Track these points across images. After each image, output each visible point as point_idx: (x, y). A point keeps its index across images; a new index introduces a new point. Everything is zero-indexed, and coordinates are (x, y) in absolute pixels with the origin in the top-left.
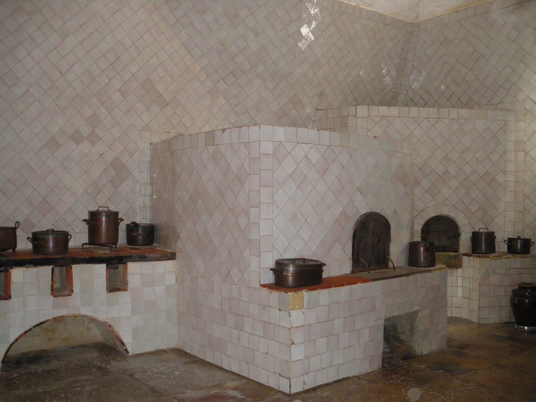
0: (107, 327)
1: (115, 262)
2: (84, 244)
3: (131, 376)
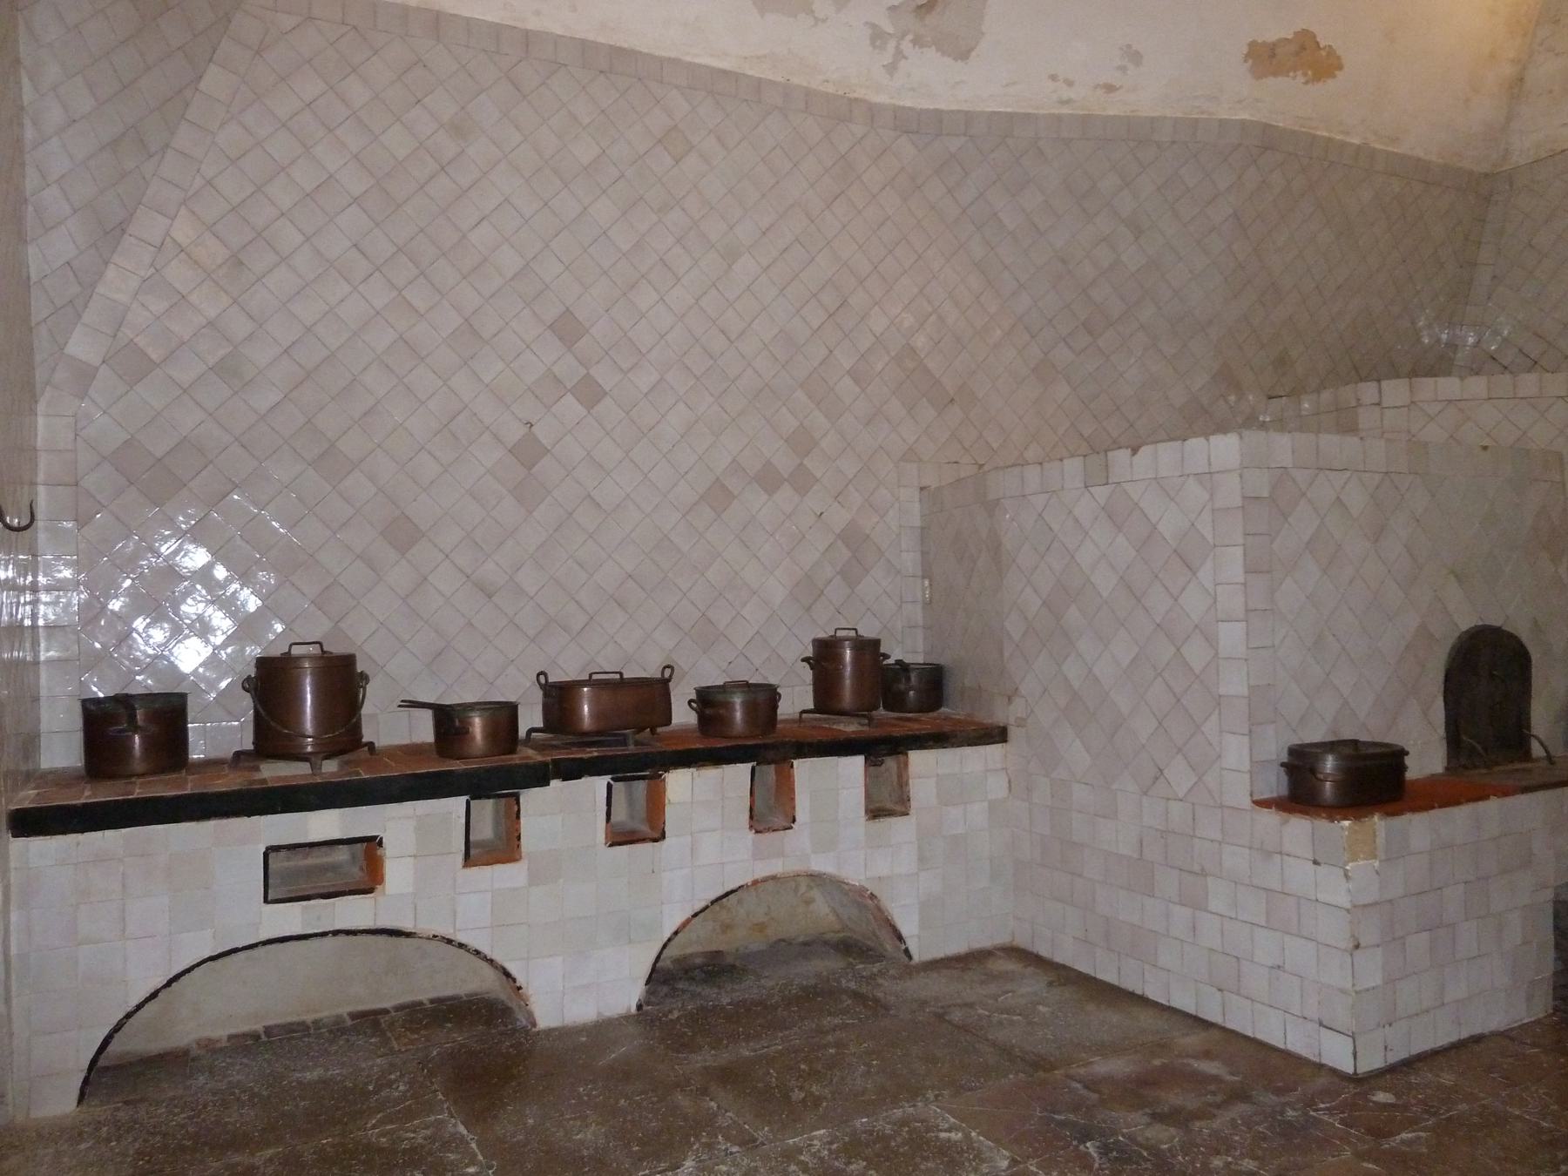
0: (866, 901)
1: (880, 749)
2: (804, 712)
3: (940, 1017)
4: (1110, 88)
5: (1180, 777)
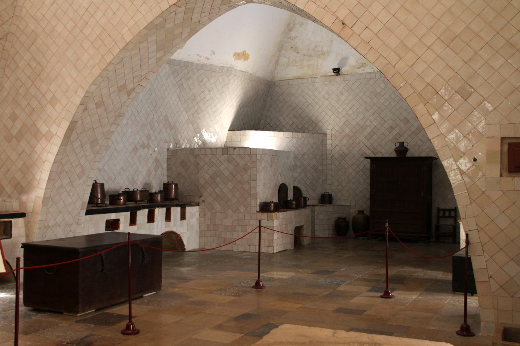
4: (208, 59)
5: (242, 209)
